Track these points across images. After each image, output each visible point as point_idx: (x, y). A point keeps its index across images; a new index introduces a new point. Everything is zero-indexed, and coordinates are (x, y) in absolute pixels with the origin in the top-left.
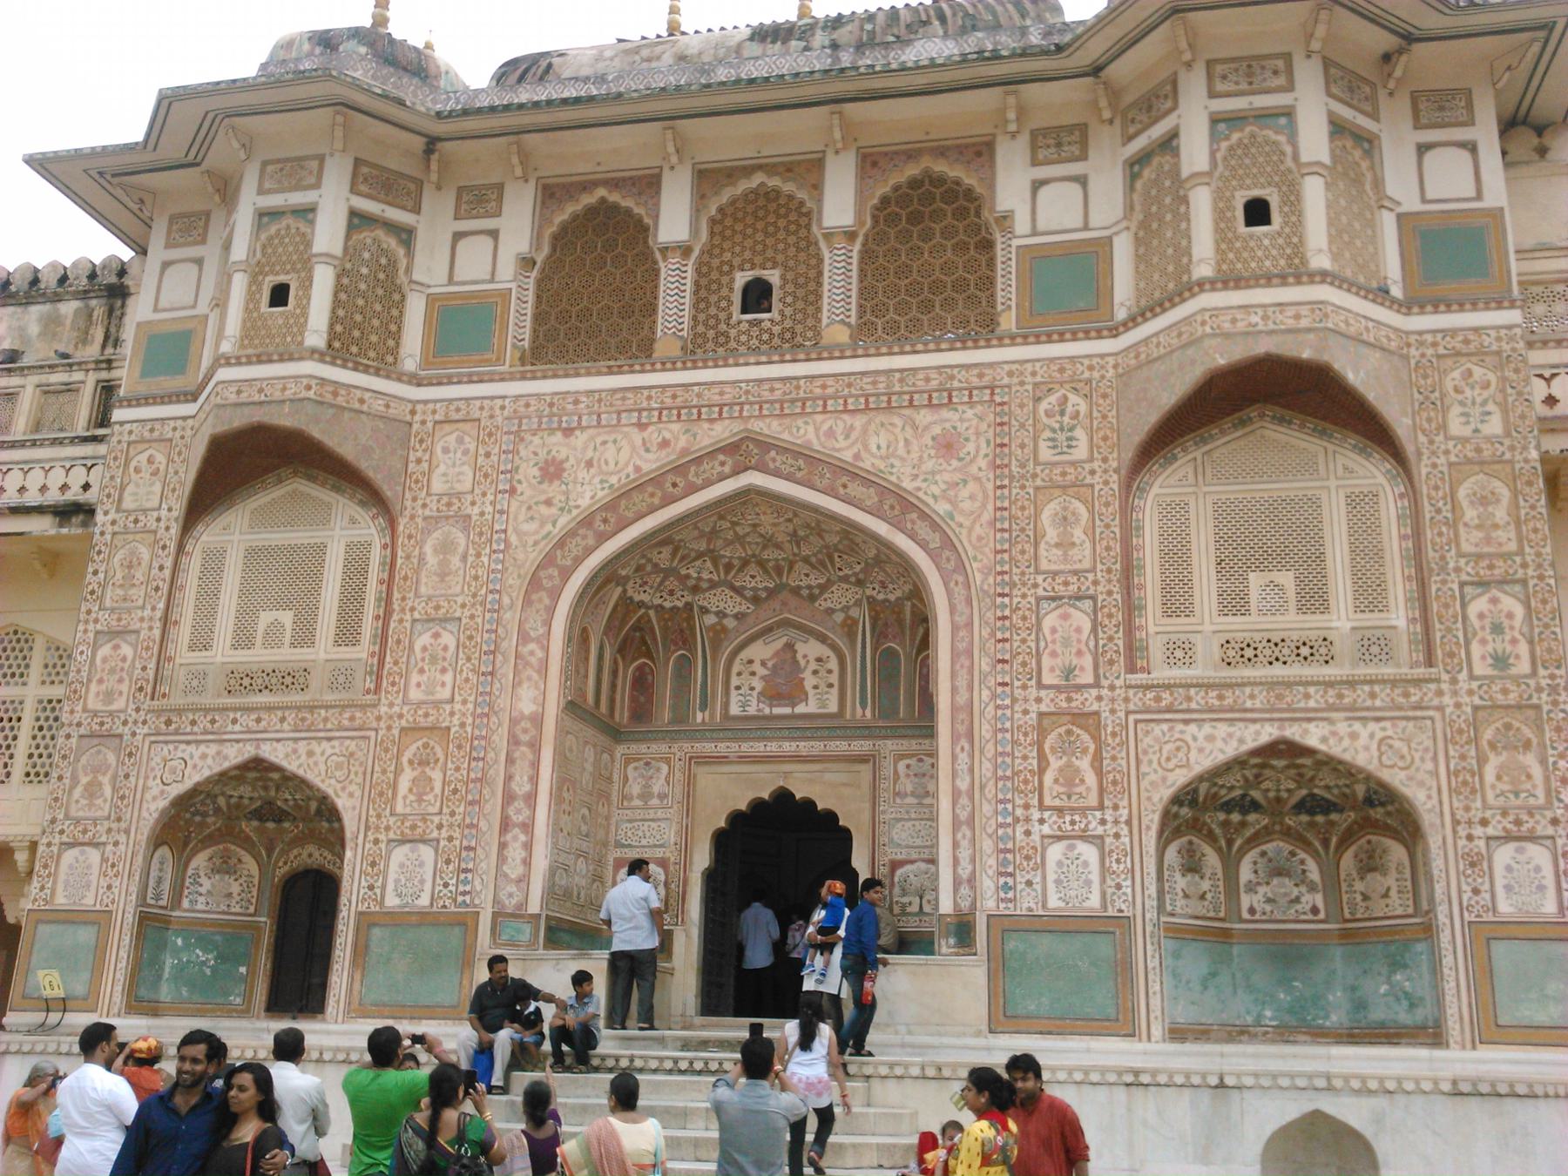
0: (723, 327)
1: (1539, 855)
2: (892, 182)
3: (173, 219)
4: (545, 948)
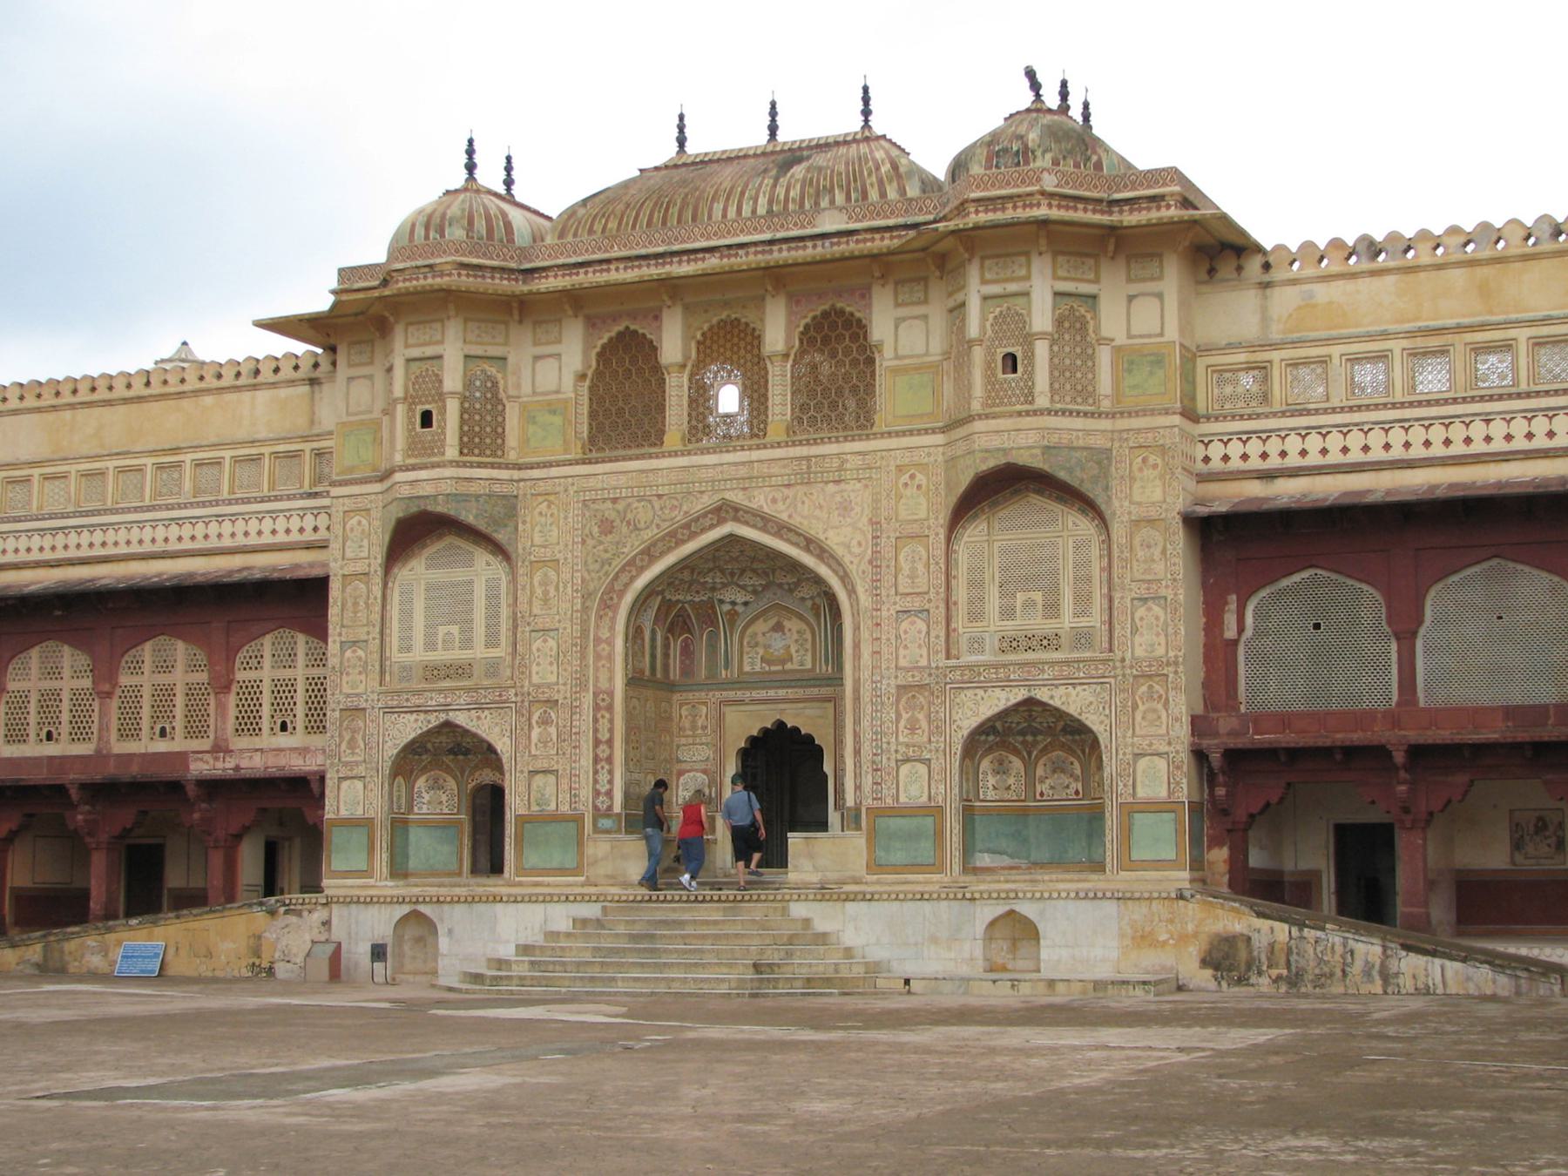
1: (1162, 764)
2: (811, 315)
4: (627, 832)
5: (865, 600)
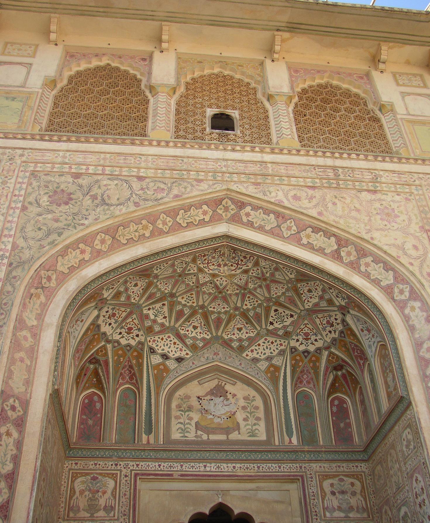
0: (199, 134)
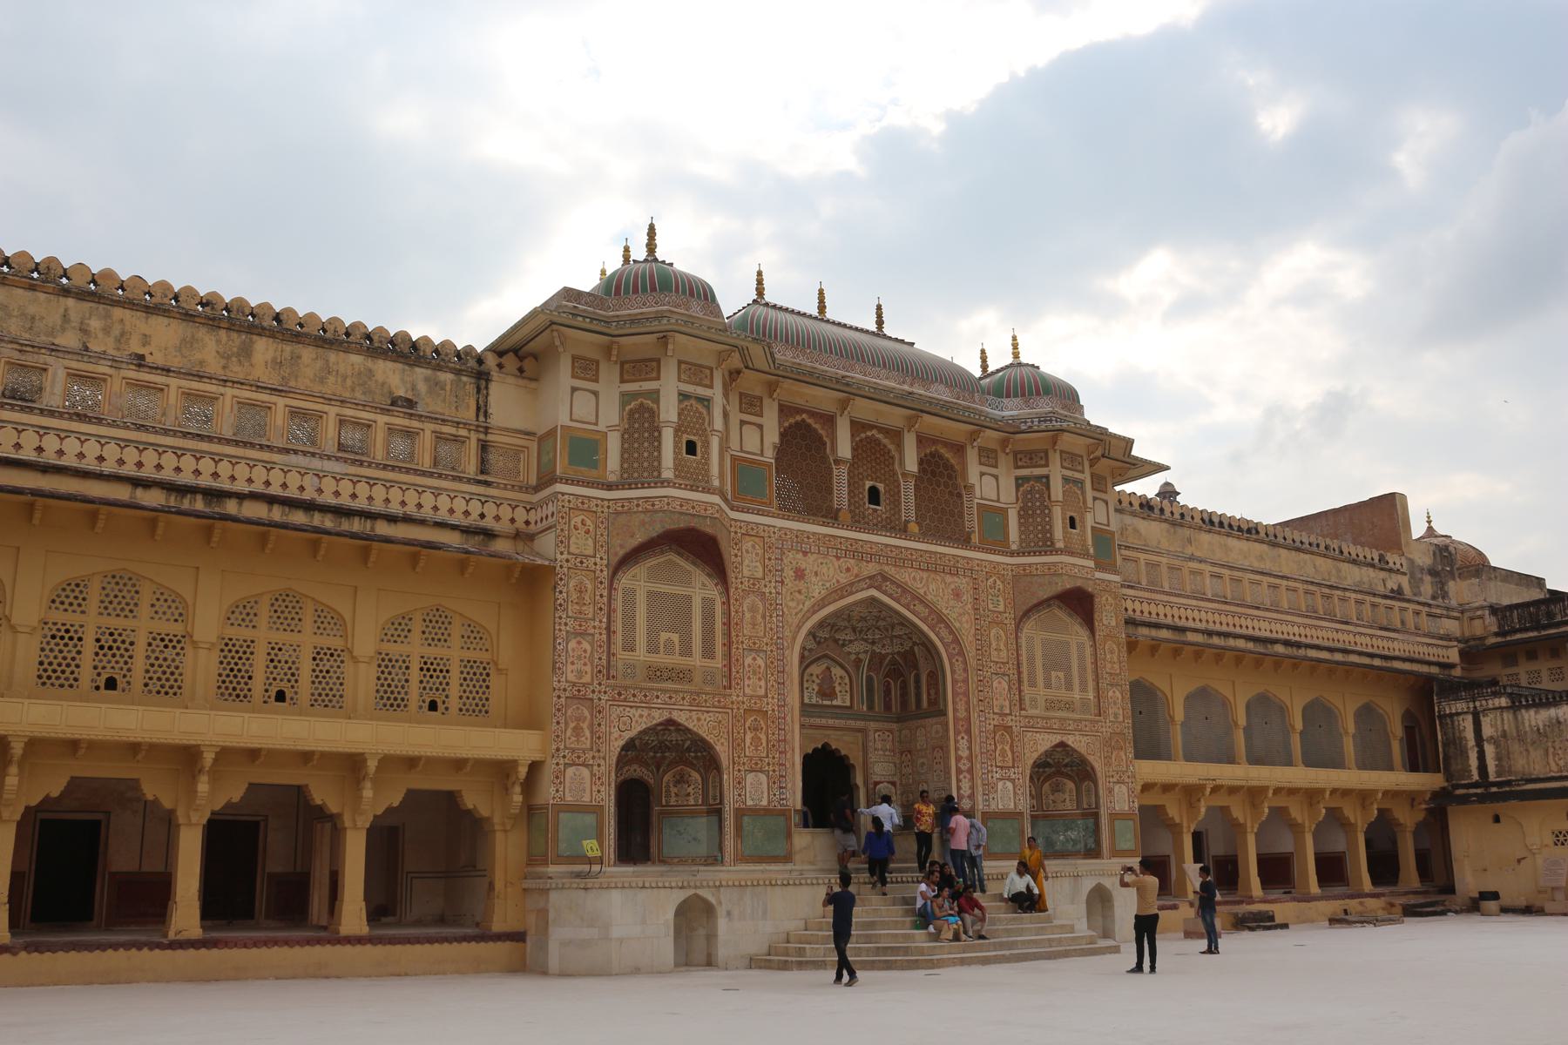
1: (1124, 788)
3: (575, 358)
5: (972, 662)
